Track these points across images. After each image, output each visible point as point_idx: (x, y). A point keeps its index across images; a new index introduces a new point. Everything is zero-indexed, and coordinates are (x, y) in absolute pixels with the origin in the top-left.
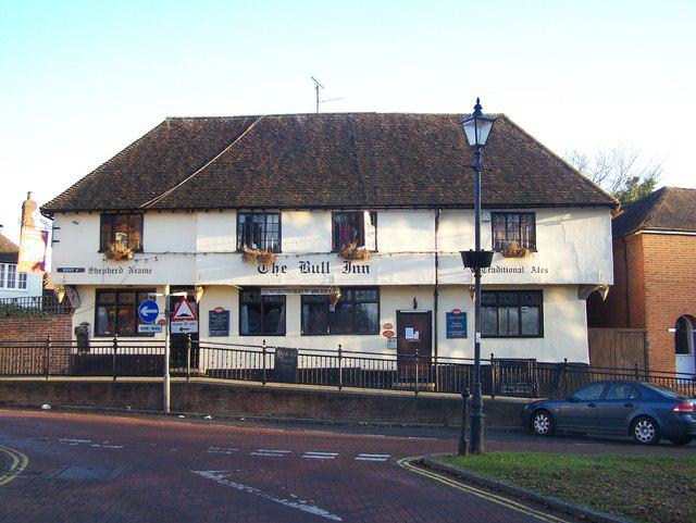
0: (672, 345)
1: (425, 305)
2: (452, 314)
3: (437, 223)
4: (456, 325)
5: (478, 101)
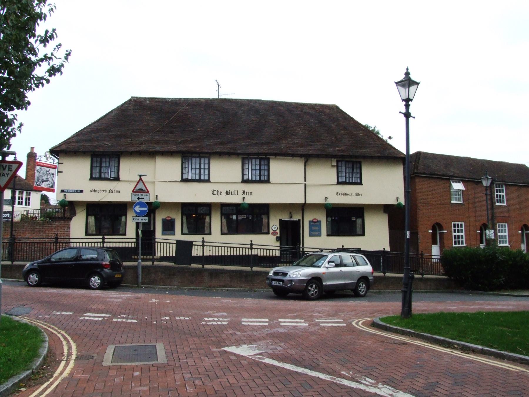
0: (430, 239)
1: (296, 217)
2: (312, 221)
3: (305, 166)
4: (315, 231)
5: (407, 69)
